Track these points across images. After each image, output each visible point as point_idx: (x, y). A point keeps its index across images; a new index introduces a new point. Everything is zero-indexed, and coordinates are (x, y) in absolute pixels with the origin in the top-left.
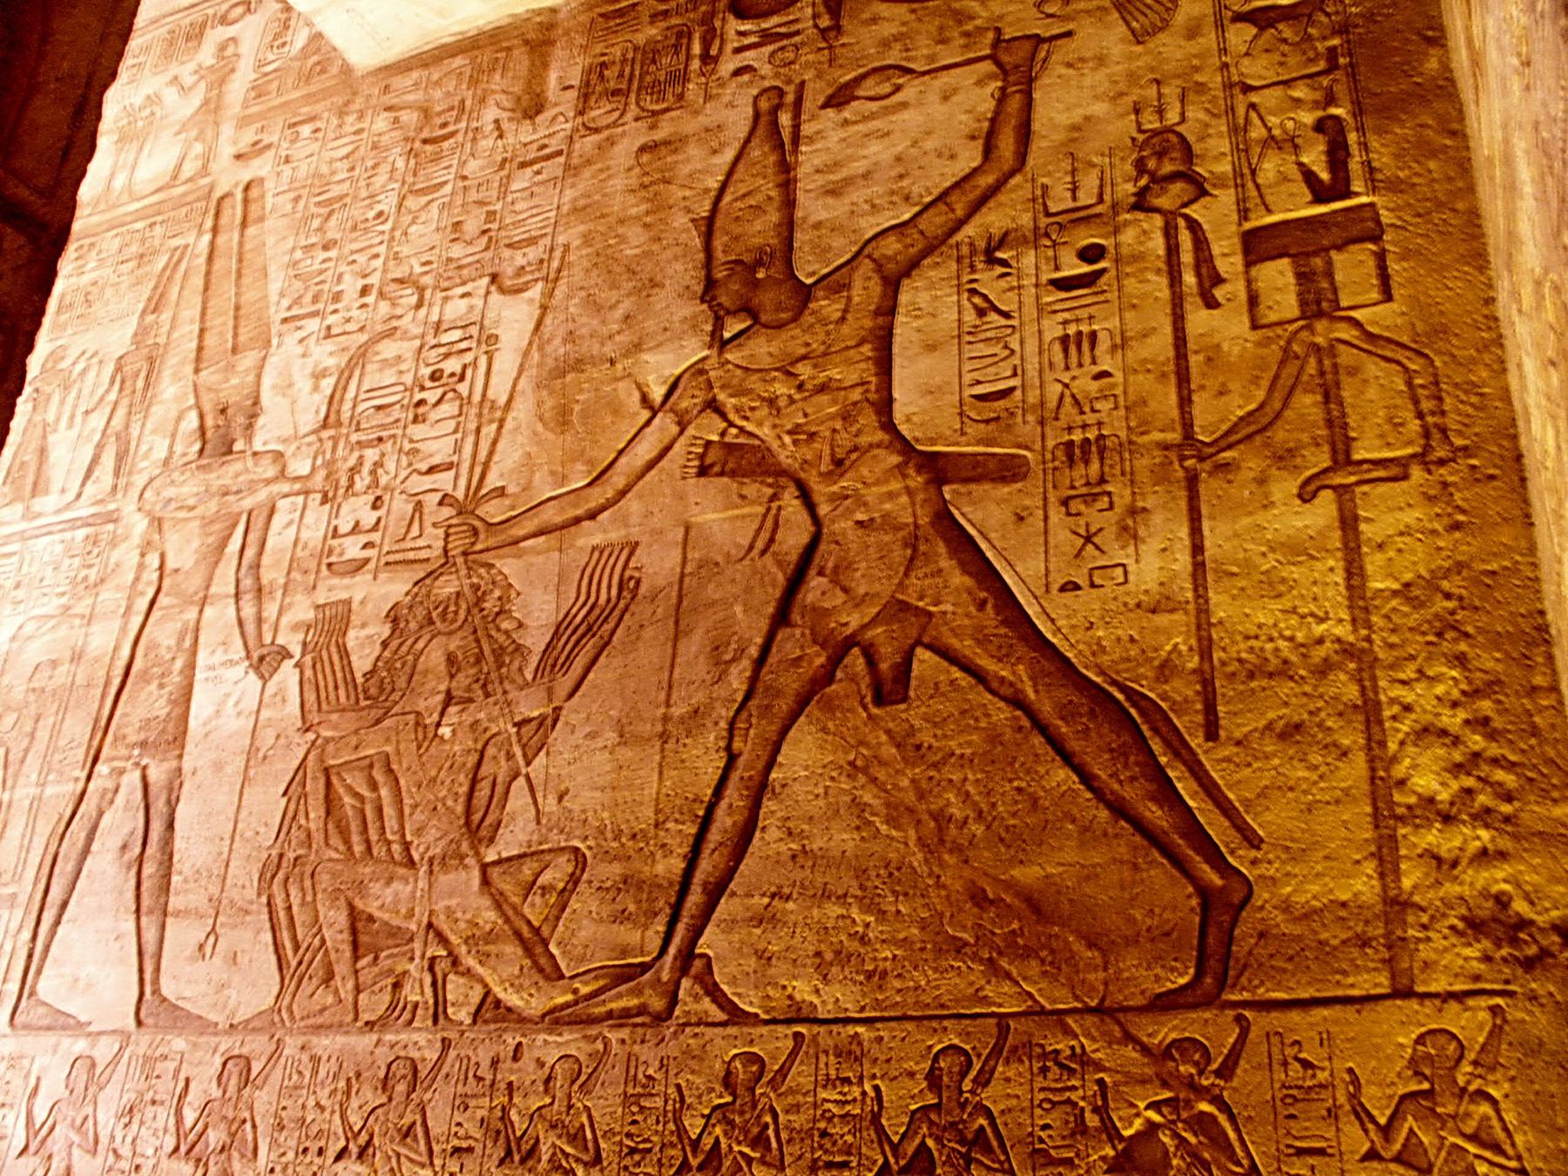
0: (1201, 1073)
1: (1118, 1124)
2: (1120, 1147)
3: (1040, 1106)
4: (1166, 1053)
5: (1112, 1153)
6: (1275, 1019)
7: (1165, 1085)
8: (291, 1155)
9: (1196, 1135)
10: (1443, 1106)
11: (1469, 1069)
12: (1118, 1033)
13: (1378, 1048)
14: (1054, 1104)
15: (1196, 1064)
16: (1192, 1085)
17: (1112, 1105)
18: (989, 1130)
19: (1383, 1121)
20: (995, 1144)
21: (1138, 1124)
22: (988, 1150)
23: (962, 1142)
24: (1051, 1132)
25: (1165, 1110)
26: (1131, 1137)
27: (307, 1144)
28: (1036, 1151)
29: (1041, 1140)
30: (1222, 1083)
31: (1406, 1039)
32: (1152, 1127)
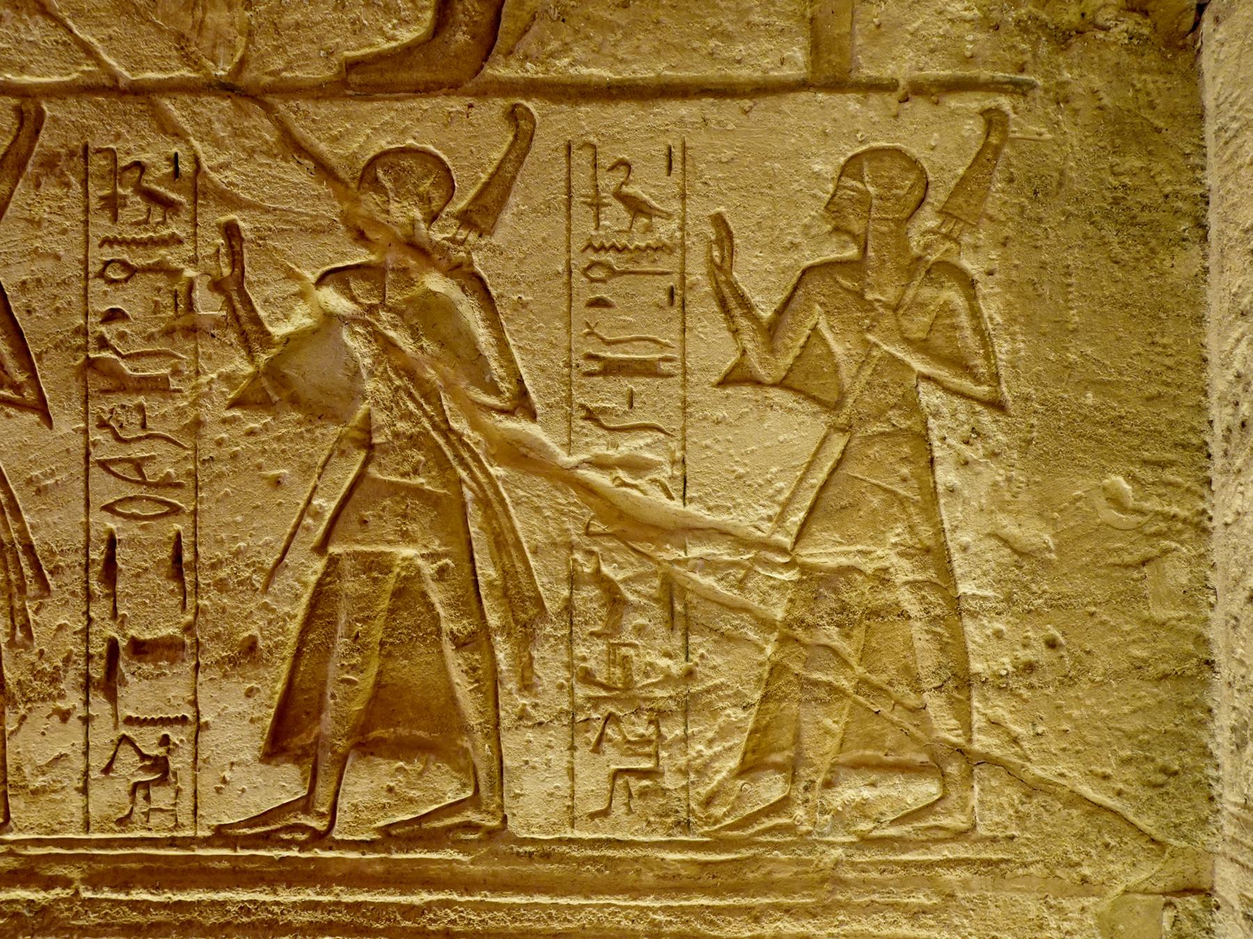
0: (432, 218)
1: (262, 313)
2: (263, 358)
3: (101, 275)
4: (368, 177)
5: (250, 369)
6: (587, 118)
7: (361, 237)
9: (415, 336)
10: (880, 287)
11: (932, 224)
12: (271, 136)
13: (772, 179)
14: (131, 271)
15: (425, 199)
16: (414, 246)
17: (250, 275)
19: (766, 314)
21: (300, 319)
24: (121, 327)
25: (357, 287)
26: (288, 339)
29: (103, 344)
30: (472, 237)
31: (826, 167)
32: (330, 319)
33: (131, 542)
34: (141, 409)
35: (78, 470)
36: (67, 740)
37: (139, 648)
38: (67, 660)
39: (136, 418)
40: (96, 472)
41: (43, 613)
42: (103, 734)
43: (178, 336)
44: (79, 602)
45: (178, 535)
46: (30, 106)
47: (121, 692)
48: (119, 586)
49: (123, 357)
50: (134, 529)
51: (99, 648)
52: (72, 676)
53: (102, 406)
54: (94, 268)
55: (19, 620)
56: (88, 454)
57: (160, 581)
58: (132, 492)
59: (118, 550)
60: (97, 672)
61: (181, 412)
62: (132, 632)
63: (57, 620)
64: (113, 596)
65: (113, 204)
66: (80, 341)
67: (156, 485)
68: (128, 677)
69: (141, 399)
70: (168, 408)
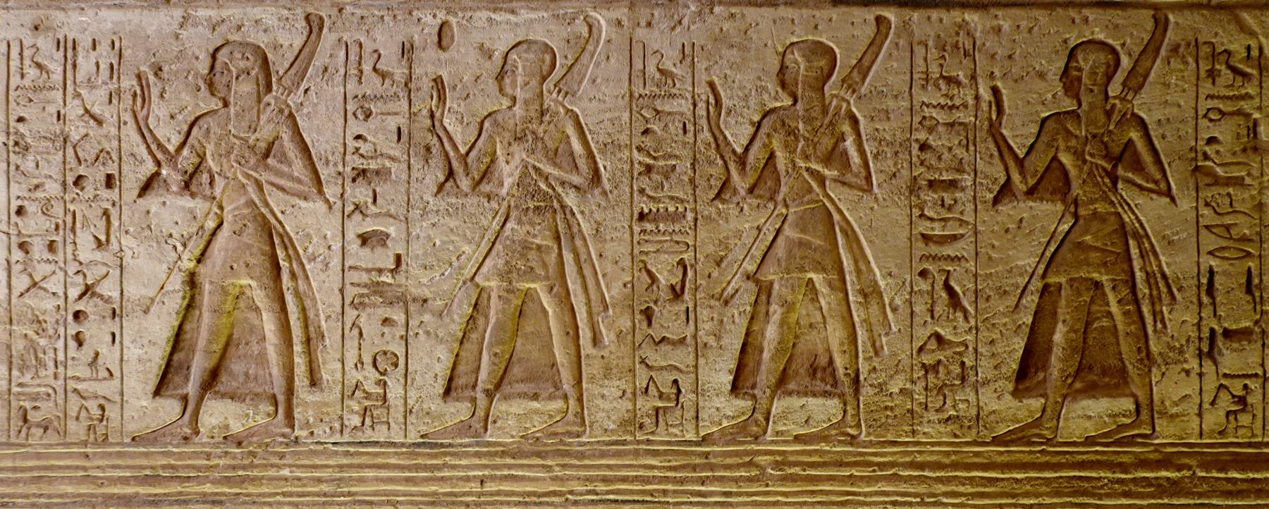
8: (53, 188)
18: (1140, 145)
20: (1147, 158)
22: (1138, 166)
23: (1107, 157)
24: (1216, 147)
27: (82, 171)
28: (1197, 168)
29: (1206, 157)
33: (1226, 273)
34: (1229, 195)
35: (1193, 231)
36: (1190, 387)
37: (1227, 334)
38: (1188, 341)
39: (1227, 201)
40: (1203, 232)
41: (1174, 313)
42: (1211, 384)
43: (1250, 152)
44: (1195, 307)
45: (1249, 270)
46: (1161, 15)
47: (1219, 359)
48: (1218, 299)
49: (1220, 165)
50: (1226, 265)
51: (1206, 333)
52: (1190, 353)
53: (1207, 194)
54: (1201, 113)
55: (1159, 318)
56: (1198, 222)
57: (1241, 295)
58: (1224, 243)
59: (1217, 278)
60: (1206, 350)
61: (1253, 198)
62: (1226, 325)
63: (1181, 319)
64: (1214, 304)
65: (1212, 74)
66: (1193, 155)
67: (1238, 240)
68: (1225, 351)
69: (1231, 190)
70: (1246, 195)
